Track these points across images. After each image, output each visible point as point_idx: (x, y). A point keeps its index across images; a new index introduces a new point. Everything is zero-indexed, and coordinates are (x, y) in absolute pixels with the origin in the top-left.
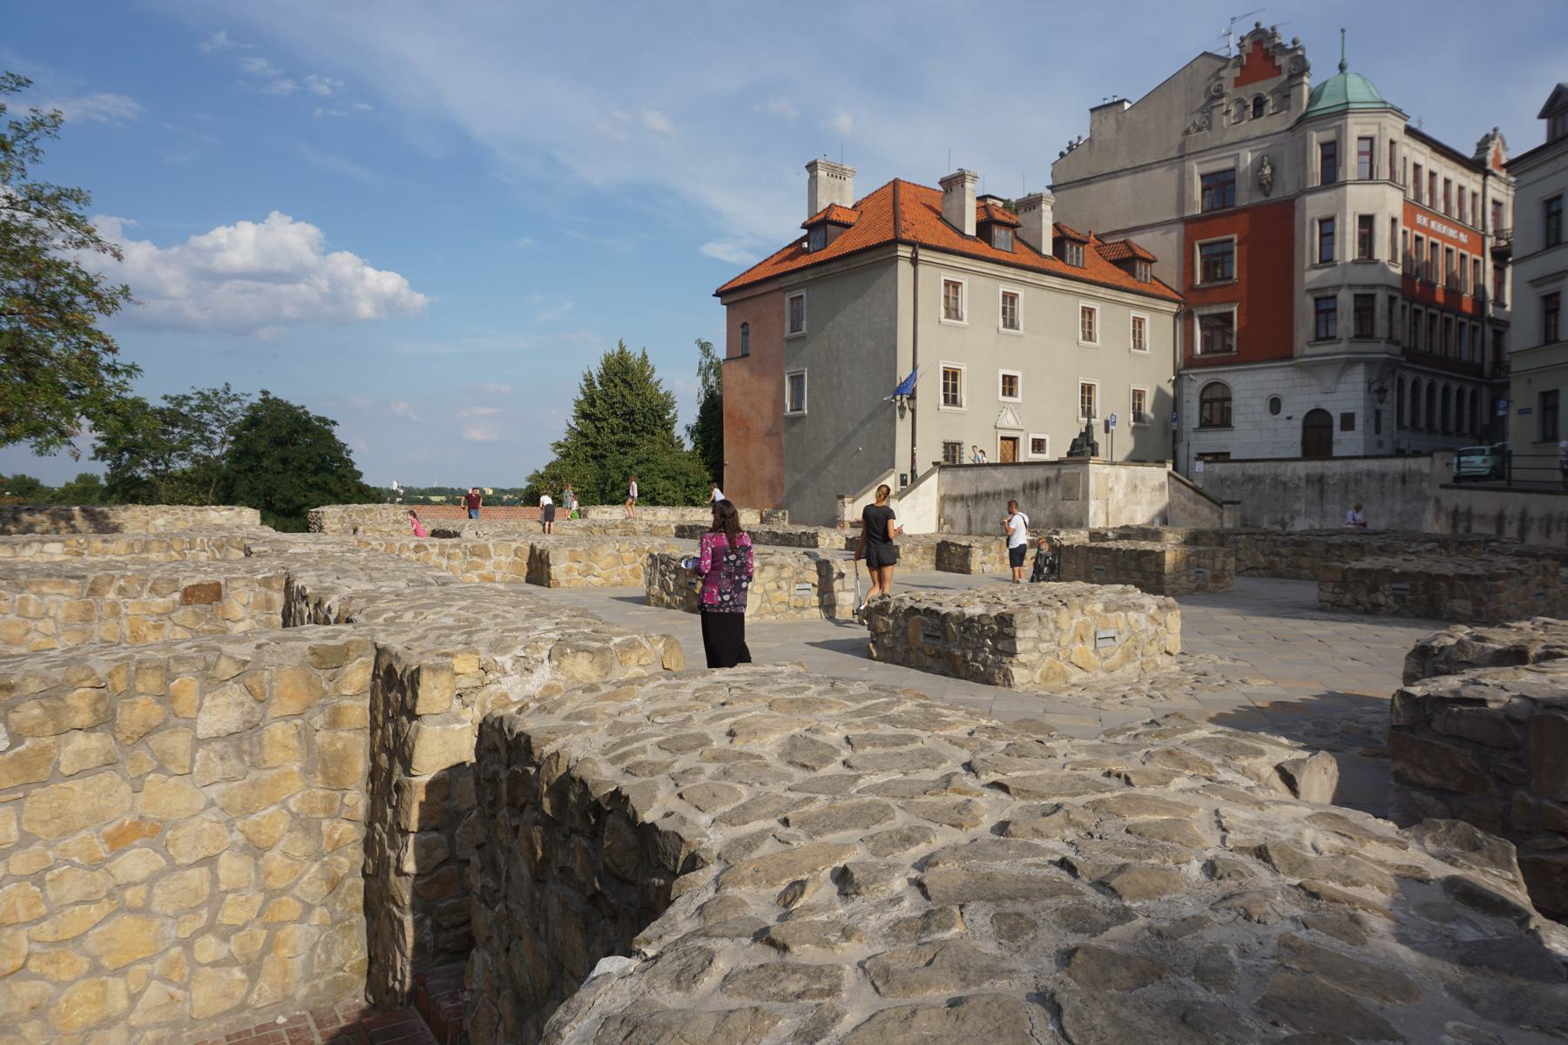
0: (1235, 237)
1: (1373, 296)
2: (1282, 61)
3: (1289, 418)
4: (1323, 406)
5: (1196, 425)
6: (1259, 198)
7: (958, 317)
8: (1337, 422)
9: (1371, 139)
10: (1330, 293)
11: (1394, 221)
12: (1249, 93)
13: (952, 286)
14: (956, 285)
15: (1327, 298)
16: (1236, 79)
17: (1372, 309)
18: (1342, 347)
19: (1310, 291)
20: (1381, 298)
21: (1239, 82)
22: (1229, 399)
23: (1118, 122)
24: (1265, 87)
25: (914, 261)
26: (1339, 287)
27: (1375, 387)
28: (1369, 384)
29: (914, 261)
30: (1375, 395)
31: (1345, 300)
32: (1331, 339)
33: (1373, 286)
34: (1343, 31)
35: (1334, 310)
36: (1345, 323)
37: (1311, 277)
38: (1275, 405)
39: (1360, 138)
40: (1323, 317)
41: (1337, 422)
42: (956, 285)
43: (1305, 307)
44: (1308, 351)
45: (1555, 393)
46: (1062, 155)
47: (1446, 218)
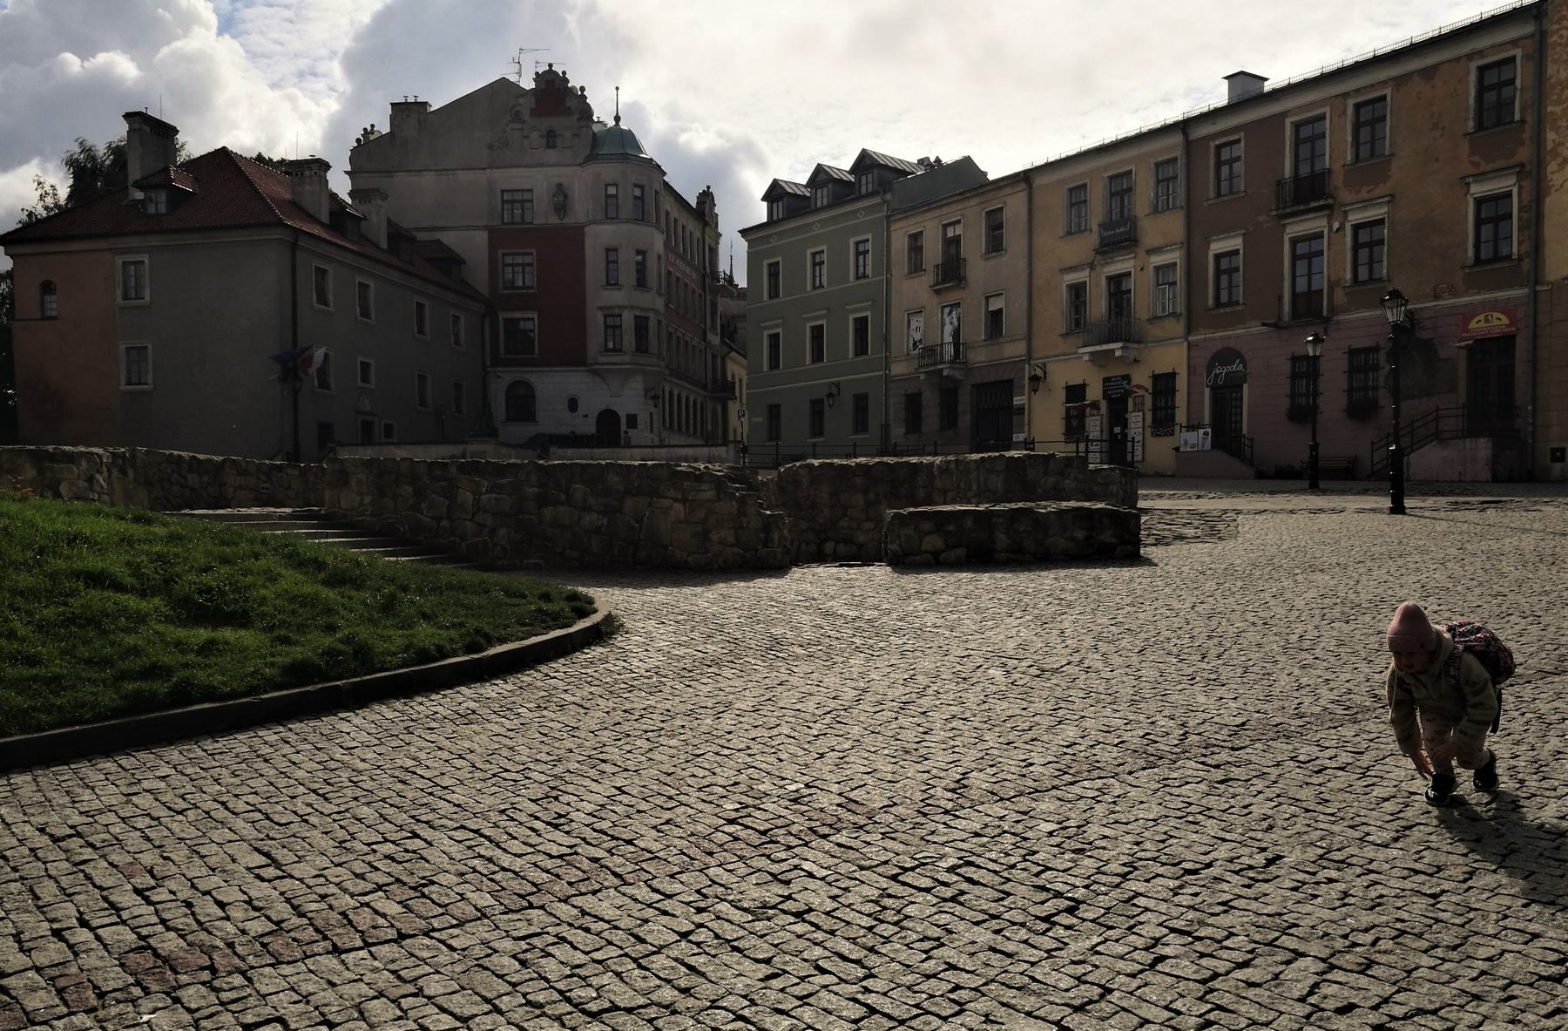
0: (534, 251)
1: (647, 319)
2: (570, 103)
3: (586, 416)
4: (613, 408)
5: (504, 419)
6: (554, 220)
7: (326, 304)
8: (623, 421)
9: (642, 187)
10: (617, 312)
11: (659, 257)
12: (546, 123)
13: (321, 273)
14: (324, 272)
15: (614, 316)
16: (532, 110)
17: (647, 329)
18: (627, 358)
19: (600, 308)
20: (652, 323)
21: (533, 113)
22: (534, 397)
23: (420, 122)
24: (556, 123)
25: (294, 247)
26: (623, 307)
27: (651, 394)
28: (647, 391)
29: (294, 247)
30: (651, 402)
31: (628, 318)
32: (617, 350)
33: (649, 310)
34: (617, 88)
35: (620, 327)
36: (629, 340)
37: (599, 297)
38: (573, 405)
39: (636, 186)
40: (610, 331)
41: (623, 421)
42: (324, 272)
43: (595, 320)
44: (601, 359)
45: (778, 406)
46: (358, 140)
47: (683, 259)
